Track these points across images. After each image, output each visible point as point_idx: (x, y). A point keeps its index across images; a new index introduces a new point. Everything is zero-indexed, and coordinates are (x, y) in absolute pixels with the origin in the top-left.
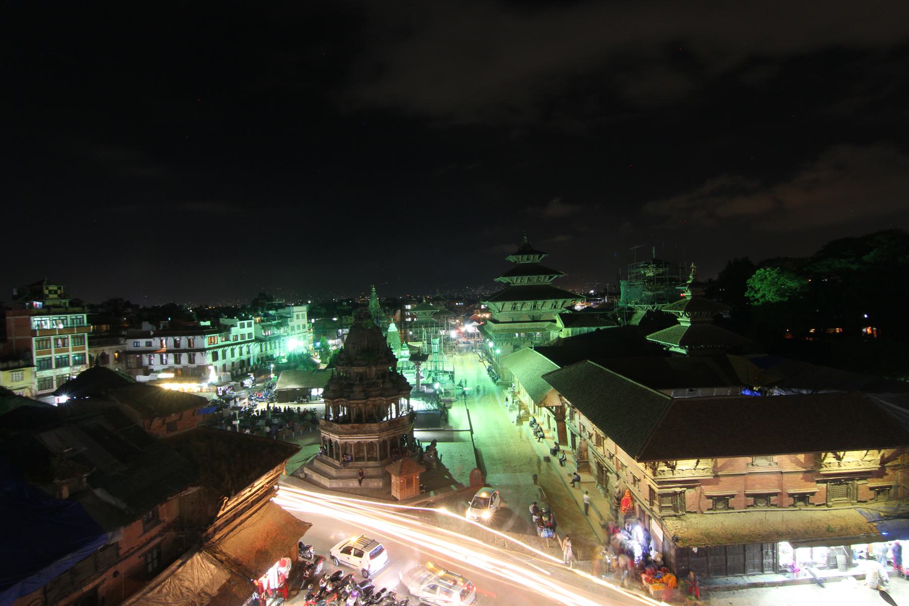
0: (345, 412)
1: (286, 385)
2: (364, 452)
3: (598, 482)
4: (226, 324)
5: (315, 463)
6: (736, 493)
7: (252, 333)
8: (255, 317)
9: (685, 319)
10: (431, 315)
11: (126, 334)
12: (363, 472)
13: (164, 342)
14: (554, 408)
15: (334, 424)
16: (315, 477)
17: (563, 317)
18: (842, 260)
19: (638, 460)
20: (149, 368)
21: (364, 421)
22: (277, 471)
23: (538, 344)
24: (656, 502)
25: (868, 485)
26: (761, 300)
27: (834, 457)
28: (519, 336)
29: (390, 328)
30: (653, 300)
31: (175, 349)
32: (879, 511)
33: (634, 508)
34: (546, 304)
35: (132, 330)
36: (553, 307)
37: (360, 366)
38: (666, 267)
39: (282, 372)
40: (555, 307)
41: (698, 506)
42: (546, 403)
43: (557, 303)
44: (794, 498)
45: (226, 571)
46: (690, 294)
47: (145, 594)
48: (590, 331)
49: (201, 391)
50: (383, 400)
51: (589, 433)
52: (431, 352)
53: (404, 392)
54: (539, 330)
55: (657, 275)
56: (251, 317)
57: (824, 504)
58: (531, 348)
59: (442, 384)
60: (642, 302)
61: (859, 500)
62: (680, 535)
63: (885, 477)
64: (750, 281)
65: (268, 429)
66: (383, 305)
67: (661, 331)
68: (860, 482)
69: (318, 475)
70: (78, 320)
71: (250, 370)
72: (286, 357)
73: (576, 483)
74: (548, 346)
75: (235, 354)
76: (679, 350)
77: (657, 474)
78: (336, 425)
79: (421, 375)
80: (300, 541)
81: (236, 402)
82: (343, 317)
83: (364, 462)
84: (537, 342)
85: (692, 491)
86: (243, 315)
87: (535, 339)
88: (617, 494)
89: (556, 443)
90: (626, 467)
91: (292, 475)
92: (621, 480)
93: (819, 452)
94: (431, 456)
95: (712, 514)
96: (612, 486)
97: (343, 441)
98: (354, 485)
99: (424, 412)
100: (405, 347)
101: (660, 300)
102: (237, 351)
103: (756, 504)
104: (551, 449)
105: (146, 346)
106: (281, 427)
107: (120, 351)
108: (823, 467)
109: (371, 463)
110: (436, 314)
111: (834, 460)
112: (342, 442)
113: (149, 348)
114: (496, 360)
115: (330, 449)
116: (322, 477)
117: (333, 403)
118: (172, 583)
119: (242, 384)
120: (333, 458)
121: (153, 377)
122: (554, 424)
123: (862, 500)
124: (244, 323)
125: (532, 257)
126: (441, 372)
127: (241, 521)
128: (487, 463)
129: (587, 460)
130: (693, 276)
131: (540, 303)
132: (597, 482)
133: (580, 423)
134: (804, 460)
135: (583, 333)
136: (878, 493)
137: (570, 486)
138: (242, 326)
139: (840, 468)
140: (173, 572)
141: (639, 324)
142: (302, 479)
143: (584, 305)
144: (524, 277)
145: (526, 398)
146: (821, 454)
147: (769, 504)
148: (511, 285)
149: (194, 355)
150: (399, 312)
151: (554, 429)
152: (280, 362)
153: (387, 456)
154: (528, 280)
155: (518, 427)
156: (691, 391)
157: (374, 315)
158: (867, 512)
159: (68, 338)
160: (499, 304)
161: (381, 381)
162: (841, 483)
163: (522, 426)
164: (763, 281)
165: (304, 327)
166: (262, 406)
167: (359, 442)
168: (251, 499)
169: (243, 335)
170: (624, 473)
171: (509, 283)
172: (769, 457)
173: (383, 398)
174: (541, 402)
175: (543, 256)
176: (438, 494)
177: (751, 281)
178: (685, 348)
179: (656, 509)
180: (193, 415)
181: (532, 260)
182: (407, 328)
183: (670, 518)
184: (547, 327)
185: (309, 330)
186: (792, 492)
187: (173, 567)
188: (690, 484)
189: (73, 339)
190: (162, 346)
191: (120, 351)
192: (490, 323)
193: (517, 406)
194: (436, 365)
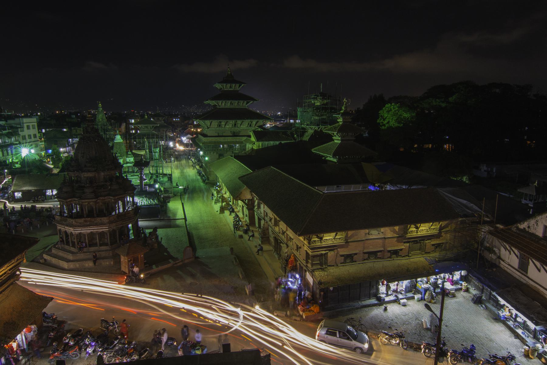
0: (78, 209)
1: (22, 187)
2: (96, 240)
3: (275, 250)
6: (358, 252)
9: (337, 138)
10: (152, 128)
12: (96, 255)
14: (247, 200)
15: (68, 219)
16: (54, 261)
17: (255, 132)
18: (437, 100)
19: (298, 234)
21: (95, 215)
22: (18, 260)
24: (310, 261)
25: (431, 243)
26: (386, 125)
27: (414, 227)
28: (223, 147)
29: (116, 139)
30: (319, 123)
32: (436, 258)
33: (296, 265)
34: (244, 123)
36: (249, 125)
37: (89, 171)
38: (328, 99)
39: (16, 176)
40: (250, 126)
43: (252, 122)
46: (342, 120)
48: (275, 144)
50: (111, 199)
51: (270, 218)
52: (152, 159)
53: (129, 192)
54: (238, 143)
55: (322, 105)
57: (407, 256)
58: (232, 156)
59: (162, 184)
60: (311, 123)
62: (323, 281)
63: (441, 238)
64: (381, 112)
66: (109, 119)
67: (322, 146)
68: (427, 242)
72: (19, 163)
73: (260, 252)
74: (246, 155)
76: (332, 159)
77: (311, 243)
78: (70, 219)
79: (144, 177)
80: (43, 311)
82: (72, 128)
83: (96, 248)
84: (237, 152)
85: (332, 253)
87: (235, 150)
88: (286, 257)
90: (293, 239)
92: (289, 248)
94: (153, 239)
95: (343, 266)
96: (283, 252)
98: (88, 266)
99: (147, 207)
100: (130, 155)
101: (323, 122)
103: (369, 258)
106: (19, 223)
108: (408, 234)
110: (156, 127)
111: (415, 229)
112: (77, 233)
114: (205, 165)
115: (66, 239)
117: (67, 202)
120: (69, 246)
122: (246, 212)
123: (428, 252)
125: (234, 86)
126: (161, 174)
128: (196, 242)
129: (268, 236)
130: (344, 108)
131: (239, 122)
132: (274, 250)
133: (264, 210)
134: (398, 230)
135: (270, 146)
136: (436, 247)
137: (256, 254)
139: (417, 234)
141: (308, 140)
142: (42, 264)
143: (272, 124)
145: (227, 195)
146: (408, 226)
147: (376, 258)
150: (123, 126)
151: (247, 215)
153: (117, 241)
154: (230, 104)
155: (222, 215)
156: (338, 187)
157: (102, 127)
158: (429, 259)
160: (208, 122)
161: (108, 184)
163: (224, 214)
165: (35, 136)
167: (91, 232)
170: (291, 243)
171: (215, 105)
172: (378, 229)
173: (111, 197)
174: (238, 197)
176: (159, 267)
177: (382, 112)
178: (336, 158)
179: (309, 265)
181: (233, 88)
182: (131, 139)
183: (318, 270)
184: (244, 141)
185: (41, 139)
186: (390, 250)
188: (331, 248)
192: (200, 136)
193: (220, 200)
194: (157, 169)
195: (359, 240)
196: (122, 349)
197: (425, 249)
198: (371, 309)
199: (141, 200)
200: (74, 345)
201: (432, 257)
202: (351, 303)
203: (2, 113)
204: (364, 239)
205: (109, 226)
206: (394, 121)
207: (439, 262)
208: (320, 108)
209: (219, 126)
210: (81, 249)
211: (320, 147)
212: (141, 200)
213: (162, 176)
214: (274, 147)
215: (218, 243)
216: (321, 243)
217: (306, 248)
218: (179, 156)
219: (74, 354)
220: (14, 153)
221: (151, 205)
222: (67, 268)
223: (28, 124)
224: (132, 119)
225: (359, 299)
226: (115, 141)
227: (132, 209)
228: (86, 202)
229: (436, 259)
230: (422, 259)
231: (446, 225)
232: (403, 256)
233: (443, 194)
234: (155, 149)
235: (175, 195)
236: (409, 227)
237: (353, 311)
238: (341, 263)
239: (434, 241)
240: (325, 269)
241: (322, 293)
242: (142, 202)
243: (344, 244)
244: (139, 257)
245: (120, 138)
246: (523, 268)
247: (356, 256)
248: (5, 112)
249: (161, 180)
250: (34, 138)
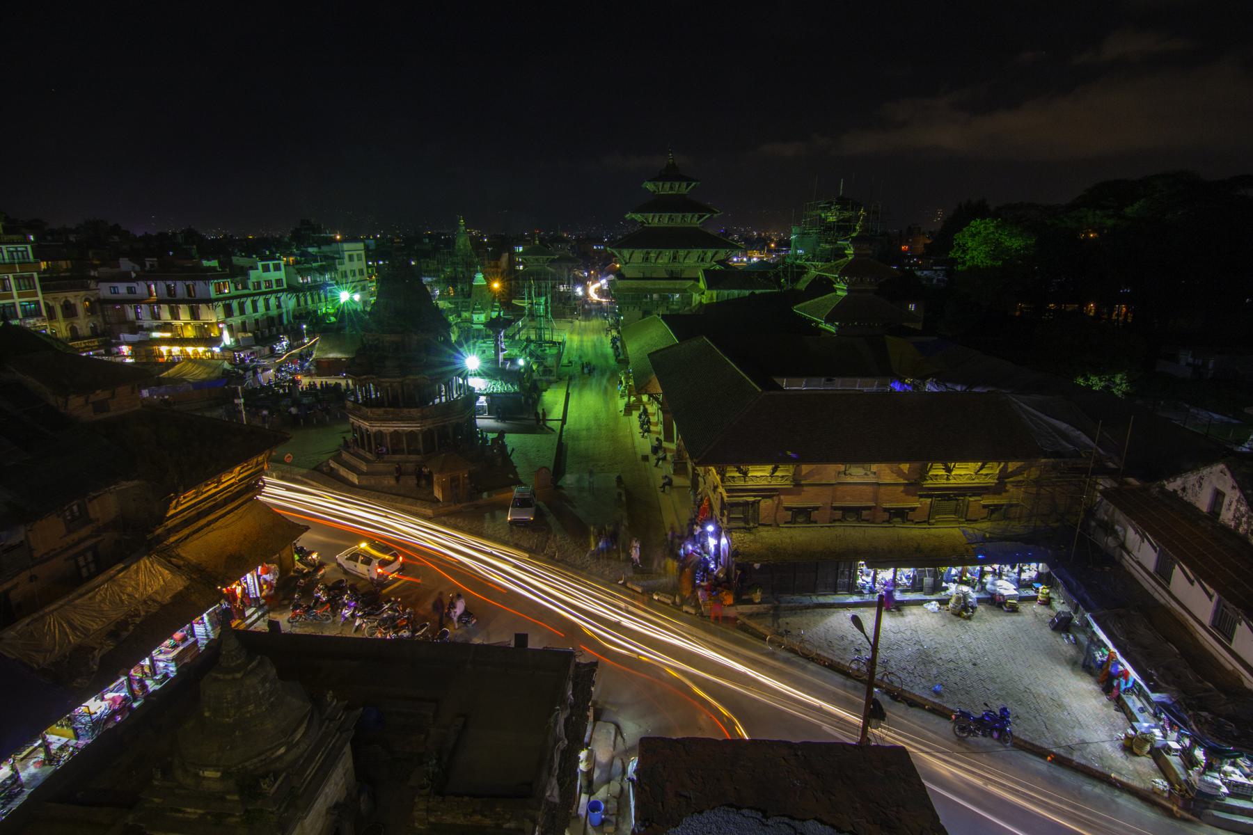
1: (327, 353)
4: (242, 264)
5: (343, 455)
7: (282, 279)
8: (284, 257)
11: (96, 275)
13: (153, 286)
16: (343, 472)
18: (1098, 212)
20: (137, 324)
23: (675, 310)
24: (726, 512)
25: (981, 502)
26: (968, 264)
27: (943, 469)
31: (169, 298)
34: (691, 254)
35: (104, 270)
36: (700, 259)
38: (852, 210)
40: (702, 260)
41: (773, 518)
42: (649, 389)
43: (705, 254)
44: (890, 513)
45: (184, 577)
46: (852, 252)
47: (73, 600)
49: (213, 358)
54: (677, 291)
55: (838, 222)
56: (279, 257)
57: (925, 522)
58: (659, 315)
59: (539, 359)
61: (968, 518)
62: (741, 550)
63: (1004, 494)
65: (294, 410)
66: (477, 244)
67: (812, 301)
68: (971, 499)
69: (344, 469)
70: (20, 253)
71: (282, 329)
73: (666, 487)
74: (689, 313)
75: (259, 309)
81: (255, 373)
82: (422, 260)
85: (769, 501)
86: (268, 253)
87: (673, 304)
89: (658, 439)
91: (315, 469)
93: (925, 462)
95: (791, 527)
97: (374, 429)
98: (388, 483)
100: (496, 307)
102: (261, 303)
103: (845, 519)
104: (652, 446)
105: (129, 293)
107: (92, 299)
108: (927, 480)
109: (413, 457)
110: (553, 261)
111: (943, 472)
113: (132, 296)
115: (364, 441)
116: (349, 472)
117: (359, 380)
118: (109, 589)
119: (272, 350)
120: (364, 449)
121: (142, 337)
123: (973, 518)
124: (268, 265)
125: (677, 186)
126: (548, 342)
127: (208, 522)
130: (860, 227)
131: (682, 253)
134: (908, 471)
135: (732, 298)
136: (992, 512)
138: (266, 269)
139: (948, 482)
140: (112, 578)
141: (805, 289)
143: (763, 258)
144: (664, 214)
146: (927, 465)
147: (860, 519)
148: (645, 225)
149: (198, 308)
150: (505, 257)
152: (328, 322)
154: (669, 219)
155: (627, 418)
157: (463, 260)
158: (972, 532)
159: (8, 279)
160: (626, 253)
162: (950, 499)
163: (630, 417)
164: (974, 237)
165: (361, 272)
166: (305, 381)
167: (395, 431)
168: (220, 497)
169: (268, 281)
172: (866, 465)
175: (693, 185)
177: (961, 236)
178: (833, 324)
179: (725, 520)
180: (133, 392)
182: (511, 280)
186: (888, 507)
187: (112, 572)
188: (768, 493)
189: (17, 281)
190: (151, 294)
191: (92, 299)
193: (627, 392)
194: (541, 333)
195: (824, 482)
196: (392, 618)
197: (967, 511)
198: (834, 612)
200: (328, 601)
201: (978, 530)
202: (796, 597)
203: (322, 233)
204: (834, 482)
205: (422, 423)
206: (982, 255)
207: (990, 542)
208: (834, 227)
209: (646, 259)
210: (379, 455)
211: (808, 302)
212: (493, 383)
214: (741, 300)
215: (604, 466)
216: (745, 481)
217: (721, 489)
218: (586, 310)
219: (325, 615)
220: (329, 299)
222: (357, 483)
223: (350, 253)
224: (519, 246)
225: (814, 590)
228: (386, 382)
229: (984, 535)
230: (956, 532)
231: (1017, 468)
232: (917, 523)
233: (1020, 406)
235: (560, 379)
236: (929, 467)
237: (799, 611)
238: (786, 523)
239: (988, 499)
240: (754, 531)
241: (739, 572)
243: (791, 488)
244: (461, 477)
245: (483, 279)
246: (1163, 573)
247: (816, 512)
248: (326, 233)
250: (360, 275)
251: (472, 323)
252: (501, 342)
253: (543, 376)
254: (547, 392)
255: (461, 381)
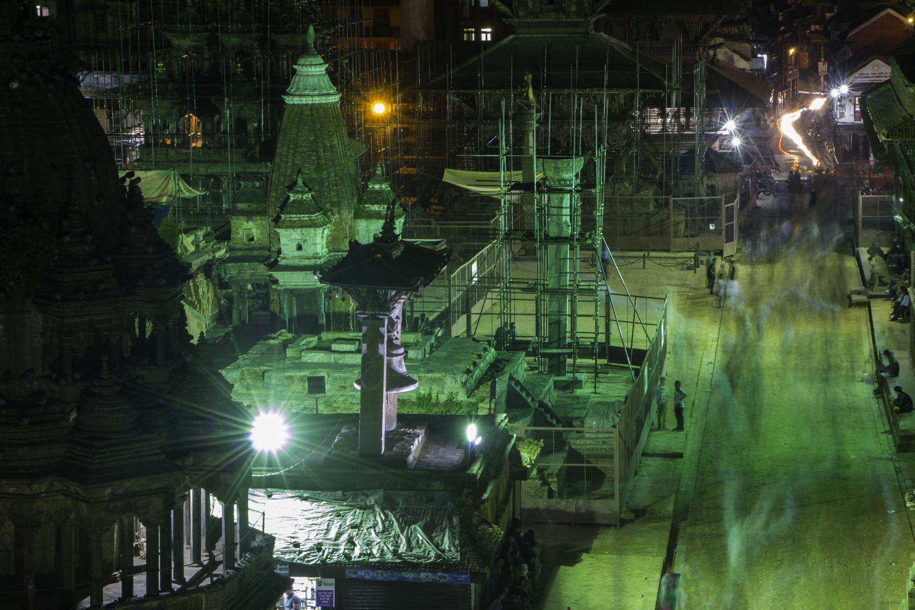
99: (380, 576)
100: (377, 198)
126: (587, 352)
173: (74, 487)
194: (560, 312)
199: (353, 527)
212: (349, 520)
213: (591, 362)
221: (406, 565)
226: (289, 100)
227: (221, 582)
234: (550, 164)
242: (351, 542)
245: (326, 79)
249: (579, 392)
251: (274, 266)
252: (391, 346)
253: (561, 495)
254: (578, 566)
255: (217, 510)
